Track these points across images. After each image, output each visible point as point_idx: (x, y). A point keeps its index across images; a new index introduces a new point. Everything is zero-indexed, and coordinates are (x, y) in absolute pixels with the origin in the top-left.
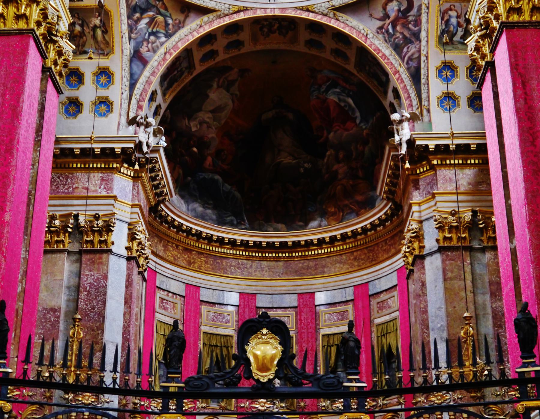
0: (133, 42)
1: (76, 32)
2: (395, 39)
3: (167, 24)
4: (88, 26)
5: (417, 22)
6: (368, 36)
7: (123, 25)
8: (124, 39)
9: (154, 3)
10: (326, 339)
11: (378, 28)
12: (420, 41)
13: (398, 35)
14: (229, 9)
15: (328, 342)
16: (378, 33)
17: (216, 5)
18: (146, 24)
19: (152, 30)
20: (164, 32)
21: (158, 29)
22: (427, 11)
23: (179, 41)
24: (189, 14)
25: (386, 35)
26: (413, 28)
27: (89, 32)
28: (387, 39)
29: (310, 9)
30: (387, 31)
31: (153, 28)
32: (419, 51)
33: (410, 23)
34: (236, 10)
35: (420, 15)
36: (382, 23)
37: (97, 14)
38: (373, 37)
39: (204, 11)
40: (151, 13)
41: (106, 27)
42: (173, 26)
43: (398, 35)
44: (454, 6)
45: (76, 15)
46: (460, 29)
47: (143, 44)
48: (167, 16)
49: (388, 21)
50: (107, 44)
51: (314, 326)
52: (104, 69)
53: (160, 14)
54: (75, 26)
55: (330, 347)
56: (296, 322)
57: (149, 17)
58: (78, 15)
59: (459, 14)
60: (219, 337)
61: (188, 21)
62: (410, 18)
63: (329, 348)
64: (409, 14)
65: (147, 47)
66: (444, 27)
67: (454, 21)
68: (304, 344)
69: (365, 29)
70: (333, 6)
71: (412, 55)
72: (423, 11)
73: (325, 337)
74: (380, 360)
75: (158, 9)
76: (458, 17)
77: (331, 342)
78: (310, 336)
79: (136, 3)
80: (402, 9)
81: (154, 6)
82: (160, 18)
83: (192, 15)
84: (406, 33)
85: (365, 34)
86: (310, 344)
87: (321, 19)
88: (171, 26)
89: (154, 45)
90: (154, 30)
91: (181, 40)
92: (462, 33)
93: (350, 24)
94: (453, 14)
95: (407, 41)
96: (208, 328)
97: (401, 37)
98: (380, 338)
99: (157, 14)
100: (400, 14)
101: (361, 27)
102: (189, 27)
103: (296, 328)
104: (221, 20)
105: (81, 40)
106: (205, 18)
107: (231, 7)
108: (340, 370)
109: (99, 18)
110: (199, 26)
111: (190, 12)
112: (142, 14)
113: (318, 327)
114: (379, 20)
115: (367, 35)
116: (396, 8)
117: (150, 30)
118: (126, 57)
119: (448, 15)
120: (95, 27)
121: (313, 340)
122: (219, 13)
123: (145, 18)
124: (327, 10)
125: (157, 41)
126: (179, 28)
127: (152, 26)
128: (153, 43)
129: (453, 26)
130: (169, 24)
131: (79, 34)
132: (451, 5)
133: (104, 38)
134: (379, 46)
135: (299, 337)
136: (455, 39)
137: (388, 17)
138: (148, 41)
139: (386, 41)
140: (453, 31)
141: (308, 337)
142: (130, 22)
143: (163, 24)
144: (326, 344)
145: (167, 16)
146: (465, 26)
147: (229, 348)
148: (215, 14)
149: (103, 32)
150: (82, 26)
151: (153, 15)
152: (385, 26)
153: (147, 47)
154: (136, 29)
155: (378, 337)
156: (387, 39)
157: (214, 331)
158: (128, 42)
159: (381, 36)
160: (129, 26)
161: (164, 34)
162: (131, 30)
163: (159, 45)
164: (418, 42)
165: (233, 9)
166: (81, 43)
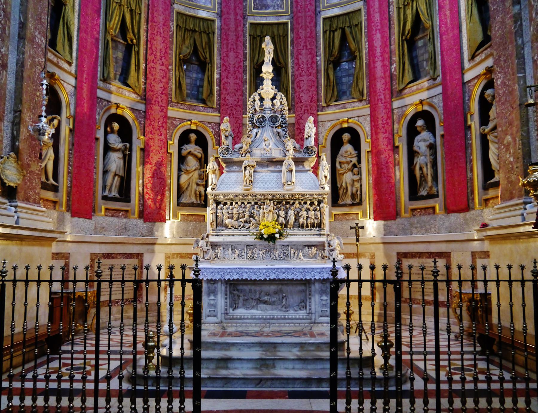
10: (328, 23)
15: (330, 26)
51: (313, 8)
55: (334, 32)
56: (292, 7)
60: (198, 21)
63: (332, 33)
68: (300, 31)
73: (327, 20)
74: (402, 38)
77: (335, 26)
78: (308, 20)
86: (309, 30)
96: (183, 7)
98: (402, 11)
103: (292, 12)
108: (344, 59)
113: (318, 9)
121: (313, 24)
135: (294, 23)
141: (306, 22)
144: (328, 28)
147: (210, 35)
155: (399, 8)
157: (191, 13)
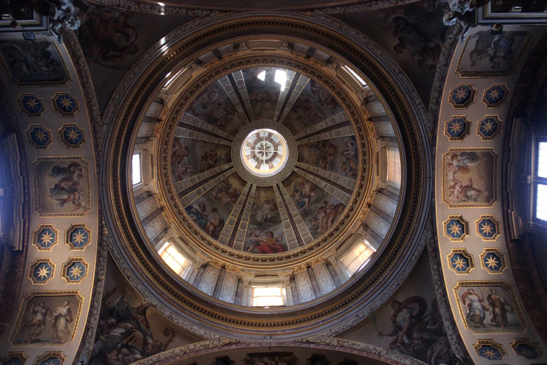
0: (99, 344)
1: (34, 321)
2: (414, 347)
3: (146, 343)
4: (51, 315)
5: (436, 318)
6: (381, 354)
7: (93, 319)
8: (90, 333)
9: (134, 315)
11: (391, 344)
12: (445, 334)
13: (416, 342)
14: (220, 340)
16: (392, 348)
17: (205, 334)
18: (121, 334)
19: (127, 343)
20: (140, 349)
21: (134, 345)
22: (444, 299)
23: (157, 362)
24: (173, 339)
25: (402, 348)
26: (433, 327)
27: (50, 321)
28: (405, 351)
29: (310, 340)
30: (403, 343)
31: (130, 341)
32: (448, 345)
33: (427, 324)
34: (227, 342)
35: (438, 308)
36: (394, 338)
37: (66, 303)
38: (387, 354)
39: (192, 338)
40: (130, 325)
41: (70, 317)
42: (153, 346)
43: (416, 342)
44: (472, 290)
45: (42, 304)
46: (487, 313)
47: (112, 352)
48: (147, 335)
49: (401, 333)
50: (68, 333)
52: (54, 354)
53: (140, 330)
54: (36, 315)
57: (126, 329)
58: (44, 304)
59: (481, 298)
61: (171, 344)
62: (426, 319)
64: (424, 316)
65: (117, 356)
66: (468, 312)
67: (477, 304)
69: (377, 348)
70: (336, 332)
71: (439, 353)
72: (439, 302)
75: (137, 321)
76: (480, 301)
79: (115, 306)
80: (414, 314)
81: (134, 319)
82: (139, 334)
83: (177, 339)
84: (426, 336)
85: (377, 353)
87: (324, 347)
88: (150, 346)
89: (126, 358)
90: (130, 344)
91: (159, 361)
92: (492, 316)
93: (358, 348)
94: (473, 297)
95: (428, 343)
97: (420, 342)
99: (137, 329)
100: (414, 320)
101: (371, 347)
102: (171, 351)
104: (210, 350)
105: (39, 329)
106: (192, 346)
107: (221, 339)
109: (67, 307)
110: (182, 353)
111: (174, 336)
112: (118, 322)
114: (390, 335)
115: (379, 353)
116: (407, 316)
117: (125, 342)
118: (87, 351)
119: (468, 299)
120: (60, 315)
122: (207, 343)
123: (122, 327)
124: (330, 338)
125: (131, 356)
126: (160, 351)
127: (128, 339)
128: (125, 355)
129: (478, 309)
130: (149, 344)
131: (38, 323)
132: (469, 290)
133: (66, 326)
134: (396, 359)
136: (484, 322)
137: (401, 329)
138: (119, 352)
139: (403, 353)
140: (480, 315)
142: (102, 323)
143: (142, 342)
145: (147, 335)
146: (491, 309)
148: (203, 343)
149: (67, 320)
150: (45, 315)
151: (132, 328)
152: (399, 340)
153: (117, 356)
154: (108, 333)
156: (405, 351)
158: (94, 337)
159: (395, 351)
160: (99, 325)
161: (141, 352)
162: (101, 330)
163: (132, 359)
164: (442, 338)
165: (224, 341)
166: (36, 332)
